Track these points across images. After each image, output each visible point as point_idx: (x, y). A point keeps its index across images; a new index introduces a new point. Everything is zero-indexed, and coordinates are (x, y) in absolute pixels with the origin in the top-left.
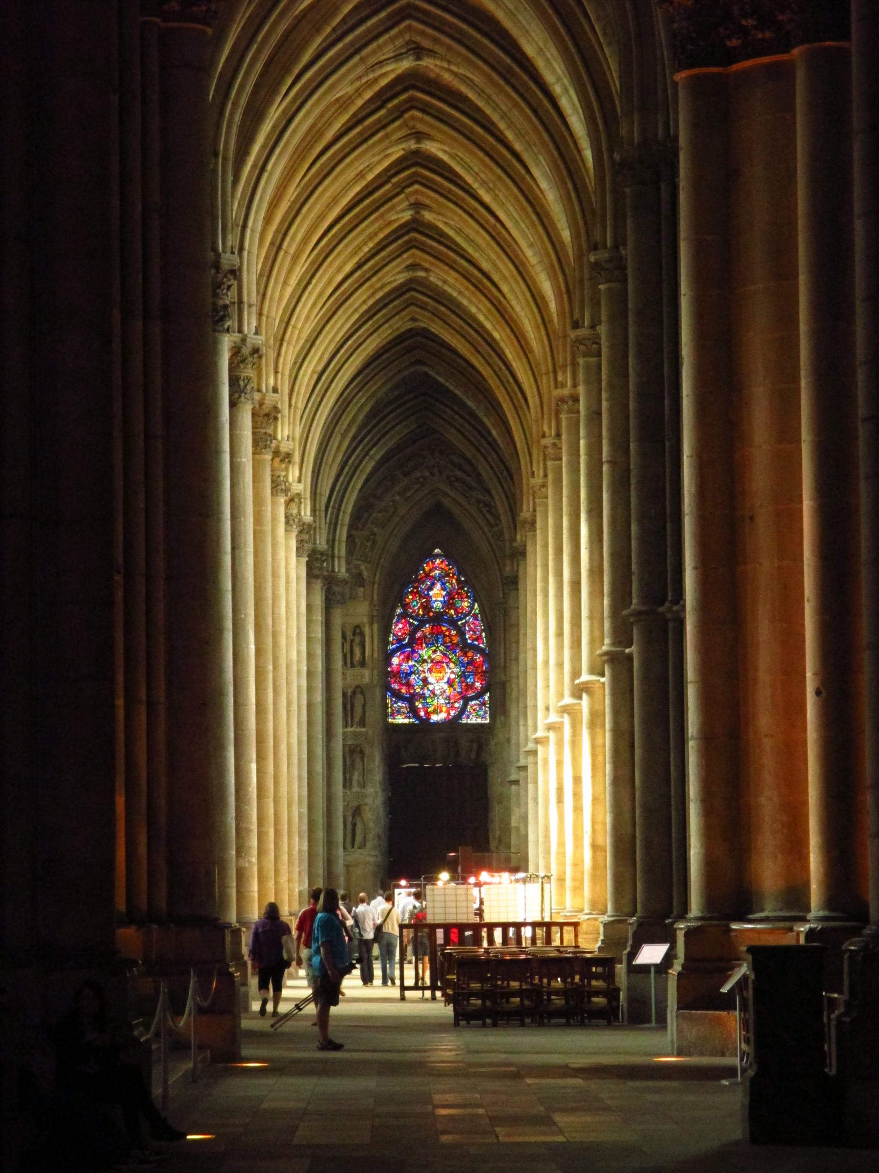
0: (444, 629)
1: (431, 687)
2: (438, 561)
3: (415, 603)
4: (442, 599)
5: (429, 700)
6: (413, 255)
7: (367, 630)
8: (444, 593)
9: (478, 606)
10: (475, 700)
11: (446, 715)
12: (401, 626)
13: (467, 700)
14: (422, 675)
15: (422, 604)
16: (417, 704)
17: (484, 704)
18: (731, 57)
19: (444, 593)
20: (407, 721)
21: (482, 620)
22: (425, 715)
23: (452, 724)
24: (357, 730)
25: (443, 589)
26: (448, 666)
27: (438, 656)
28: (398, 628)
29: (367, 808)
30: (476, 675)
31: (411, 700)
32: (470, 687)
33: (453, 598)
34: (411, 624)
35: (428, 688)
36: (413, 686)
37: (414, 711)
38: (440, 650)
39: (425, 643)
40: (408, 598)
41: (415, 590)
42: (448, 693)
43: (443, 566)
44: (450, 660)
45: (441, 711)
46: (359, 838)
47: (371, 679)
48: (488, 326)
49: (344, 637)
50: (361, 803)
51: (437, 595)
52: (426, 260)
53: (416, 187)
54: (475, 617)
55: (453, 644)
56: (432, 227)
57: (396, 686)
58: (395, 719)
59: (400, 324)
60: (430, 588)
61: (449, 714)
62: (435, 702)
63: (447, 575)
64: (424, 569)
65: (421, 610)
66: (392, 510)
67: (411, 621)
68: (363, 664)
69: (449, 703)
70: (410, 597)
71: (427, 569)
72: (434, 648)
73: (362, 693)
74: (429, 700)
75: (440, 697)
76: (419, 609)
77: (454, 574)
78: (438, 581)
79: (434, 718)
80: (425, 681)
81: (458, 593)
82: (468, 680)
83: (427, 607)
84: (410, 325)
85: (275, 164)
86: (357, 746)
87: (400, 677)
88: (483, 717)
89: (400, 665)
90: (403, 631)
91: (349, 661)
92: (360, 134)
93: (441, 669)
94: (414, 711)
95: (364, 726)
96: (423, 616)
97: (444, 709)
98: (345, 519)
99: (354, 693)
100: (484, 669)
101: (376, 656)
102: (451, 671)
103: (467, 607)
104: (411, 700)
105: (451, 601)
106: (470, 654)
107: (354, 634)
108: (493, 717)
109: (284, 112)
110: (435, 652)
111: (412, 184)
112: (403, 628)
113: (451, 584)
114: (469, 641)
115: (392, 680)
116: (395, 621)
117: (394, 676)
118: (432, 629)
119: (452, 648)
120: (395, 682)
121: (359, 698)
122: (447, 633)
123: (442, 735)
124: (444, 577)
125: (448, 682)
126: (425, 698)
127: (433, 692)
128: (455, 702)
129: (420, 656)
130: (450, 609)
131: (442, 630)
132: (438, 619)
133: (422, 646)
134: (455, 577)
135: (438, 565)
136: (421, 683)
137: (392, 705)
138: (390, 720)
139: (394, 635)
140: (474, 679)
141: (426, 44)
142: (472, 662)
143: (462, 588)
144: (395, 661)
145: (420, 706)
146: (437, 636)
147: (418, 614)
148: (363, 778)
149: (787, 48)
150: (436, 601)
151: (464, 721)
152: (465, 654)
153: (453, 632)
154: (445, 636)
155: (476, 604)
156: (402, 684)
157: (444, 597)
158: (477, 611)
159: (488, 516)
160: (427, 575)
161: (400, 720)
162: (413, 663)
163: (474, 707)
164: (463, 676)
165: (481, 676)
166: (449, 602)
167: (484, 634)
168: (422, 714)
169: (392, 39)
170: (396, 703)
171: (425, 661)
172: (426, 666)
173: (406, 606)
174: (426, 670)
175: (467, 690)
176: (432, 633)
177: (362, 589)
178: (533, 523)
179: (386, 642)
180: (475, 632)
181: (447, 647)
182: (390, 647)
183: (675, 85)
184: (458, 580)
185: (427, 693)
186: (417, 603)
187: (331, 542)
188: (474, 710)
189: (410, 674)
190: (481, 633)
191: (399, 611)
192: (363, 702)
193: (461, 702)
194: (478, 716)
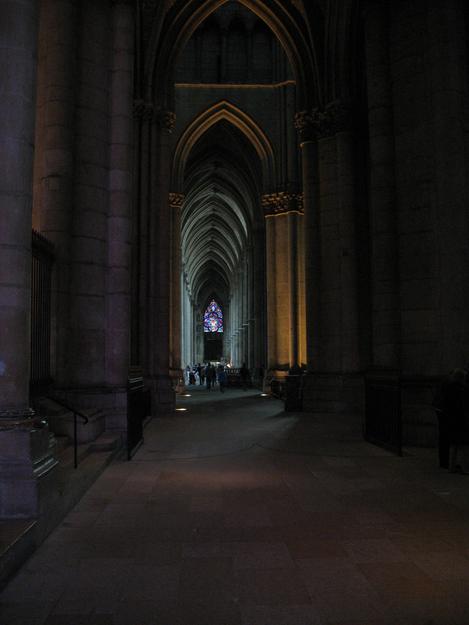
2: (213, 302)
6: (211, 247)
7: (200, 315)
8: (215, 308)
13: (219, 328)
18: (276, 213)
19: (215, 308)
20: (207, 331)
23: (216, 332)
27: (213, 319)
28: (206, 314)
31: (208, 327)
32: (219, 325)
37: (209, 330)
46: (199, 353)
47: (201, 324)
48: (224, 259)
49: (196, 316)
51: (213, 308)
52: (213, 248)
53: (212, 234)
54: (220, 312)
56: (215, 242)
57: (205, 325)
59: (208, 259)
60: (212, 307)
68: (200, 321)
73: (200, 326)
79: (213, 331)
80: (211, 324)
83: (211, 310)
84: (210, 259)
85: (188, 230)
88: (221, 331)
89: (206, 321)
91: (197, 321)
92: (203, 225)
94: (209, 330)
98: (197, 294)
102: (216, 322)
104: (208, 327)
106: (219, 319)
108: (223, 331)
109: (190, 221)
110: (213, 319)
111: (211, 234)
114: (219, 317)
119: (216, 318)
121: (199, 327)
127: (212, 326)
132: (214, 313)
135: (213, 303)
138: (204, 331)
141: (216, 209)
144: (206, 320)
145: (210, 329)
149: (286, 212)
151: (218, 332)
153: (216, 315)
160: (211, 305)
161: (207, 331)
164: (218, 323)
166: (215, 310)
168: (210, 330)
169: (209, 208)
171: (211, 320)
172: (211, 321)
173: (207, 310)
176: (212, 315)
178: (233, 295)
179: (204, 317)
182: (205, 318)
183: (265, 218)
184: (217, 306)
185: (211, 326)
187: (195, 298)
189: (208, 323)
191: (206, 311)
193: (218, 328)
194: (221, 331)
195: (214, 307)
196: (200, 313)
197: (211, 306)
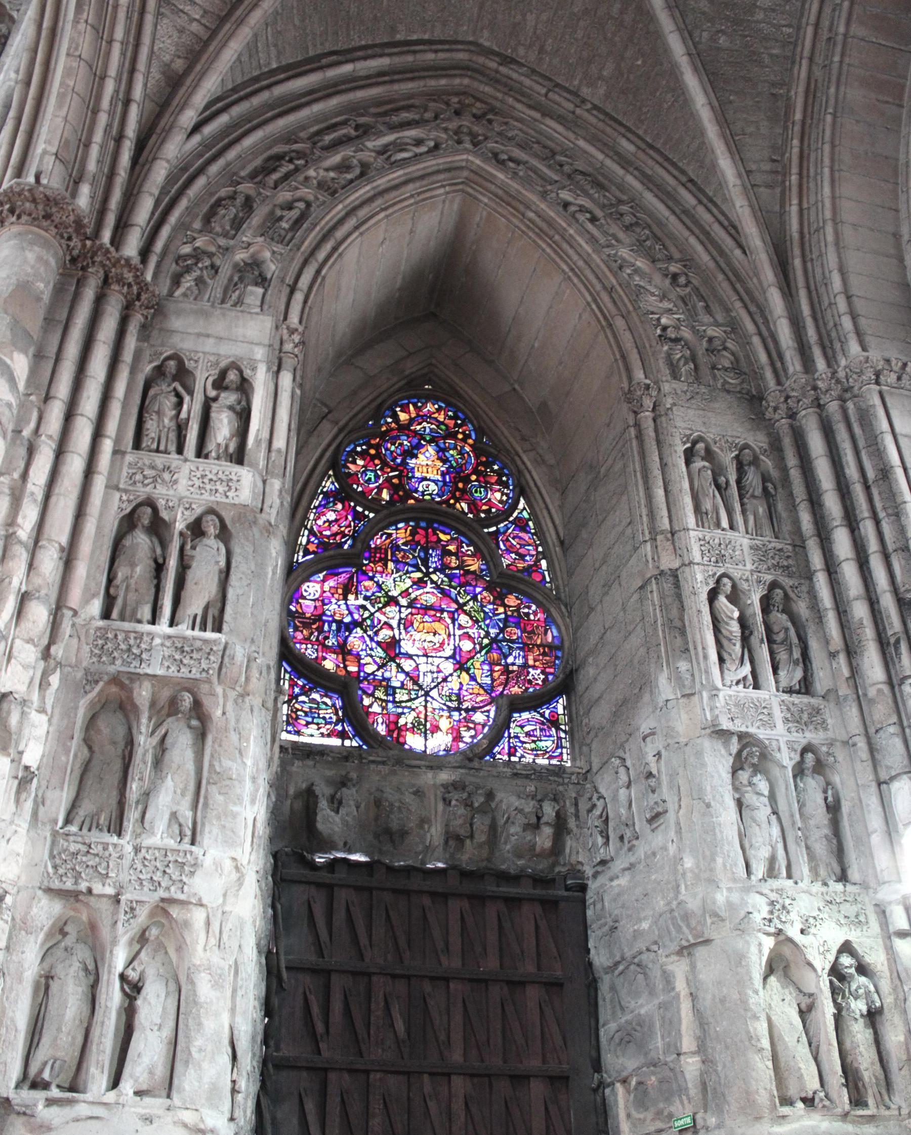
0: (443, 537)
1: (408, 665)
3: (370, 475)
4: (439, 478)
5: (401, 696)
9: (528, 502)
10: (528, 709)
11: (450, 738)
12: (331, 516)
14: (385, 634)
15: (388, 480)
16: (367, 701)
17: (554, 722)
21: (540, 533)
22: (390, 732)
24: (189, 633)
25: (444, 461)
26: (454, 620)
27: (429, 596)
29: (198, 917)
30: (530, 650)
33: (467, 480)
34: (358, 516)
35: (398, 666)
36: (358, 657)
38: (433, 582)
39: (396, 562)
40: (354, 462)
41: (372, 452)
42: (454, 684)
43: (441, 418)
44: (461, 607)
45: (436, 729)
50: (175, 893)
54: (521, 524)
55: (468, 572)
58: (298, 733)
60: (411, 453)
61: (458, 738)
62: (419, 703)
63: (453, 436)
64: (395, 417)
65: (385, 491)
66: (357, 171)
67: (359, 509)
69: (458, 709)
70: (360, 462)
71: (403, 417)
72: (419, 575)
73: (224, 534)
74: (401, 696)
75: (434, 693)
76: (380, 489)
77: (467, 437)
78: (429, 442)
79: (414, 742)
80: (392, 649)
81: (475, 471)
82: (510, 660)
86: (191, 687)
87: (320, 630)
89: (323, 601)
90: (335, 528)
93: (436, 625)
95: (218, 629)
96: (391, 502)
97: (444, 724)
99: (196, 529)
100: (550, 639)
101: (280, 442)
103: (501, 501)
105: (460, 485)
107: (220, 384)
110: (419, 583)
112: (336, 521)
113: (461, 453)
115: (299, 636)
116: (316, 503)
117: (307, 625)
118: (413, 533)
119: (466, 579)
120: (307, 640)
122: (452, 548)
123: (445, 776)
124: (445, 438)
125: (453, 657)
126: (390, 690)
128: (474, 709)
129: (379, 586)
130: (457, 500)
131: (440, 540)
133: (386, 565)
134: (470, 441)
136: (379, 652)
137: (293, 697)
139: (311, 532)
140: (525, 658)
142: (518, 619)
143: (488, 465)
144: (312, 589)
146: (425, 550)
147: (378, 499)
148: (195, 807)
150: (425, 479)
152: (500, 599)
154: (450, 553)
155: (522, 501)
156: (327, 649)
157: (443, 474)
158: (525, 515)
159: (589, 226)
162: (361, 601)
163: (527, 729)
165: (544, 654)
167: (544, 564)
170: (305, 692)
171: (392, 601)
173: (346, 479)
174: (394, 623)
175: (506, 684)
176: (412, 543)
177: (260, 291)
180: (522, 557)
181: (451, 577)
185: (397, 679)
186: (377, 477)
188: (528, 734)
190: (538, 561)
192: (223, 563)
195: (431, 450)
196: (260, 353)
197: (387, 436)
